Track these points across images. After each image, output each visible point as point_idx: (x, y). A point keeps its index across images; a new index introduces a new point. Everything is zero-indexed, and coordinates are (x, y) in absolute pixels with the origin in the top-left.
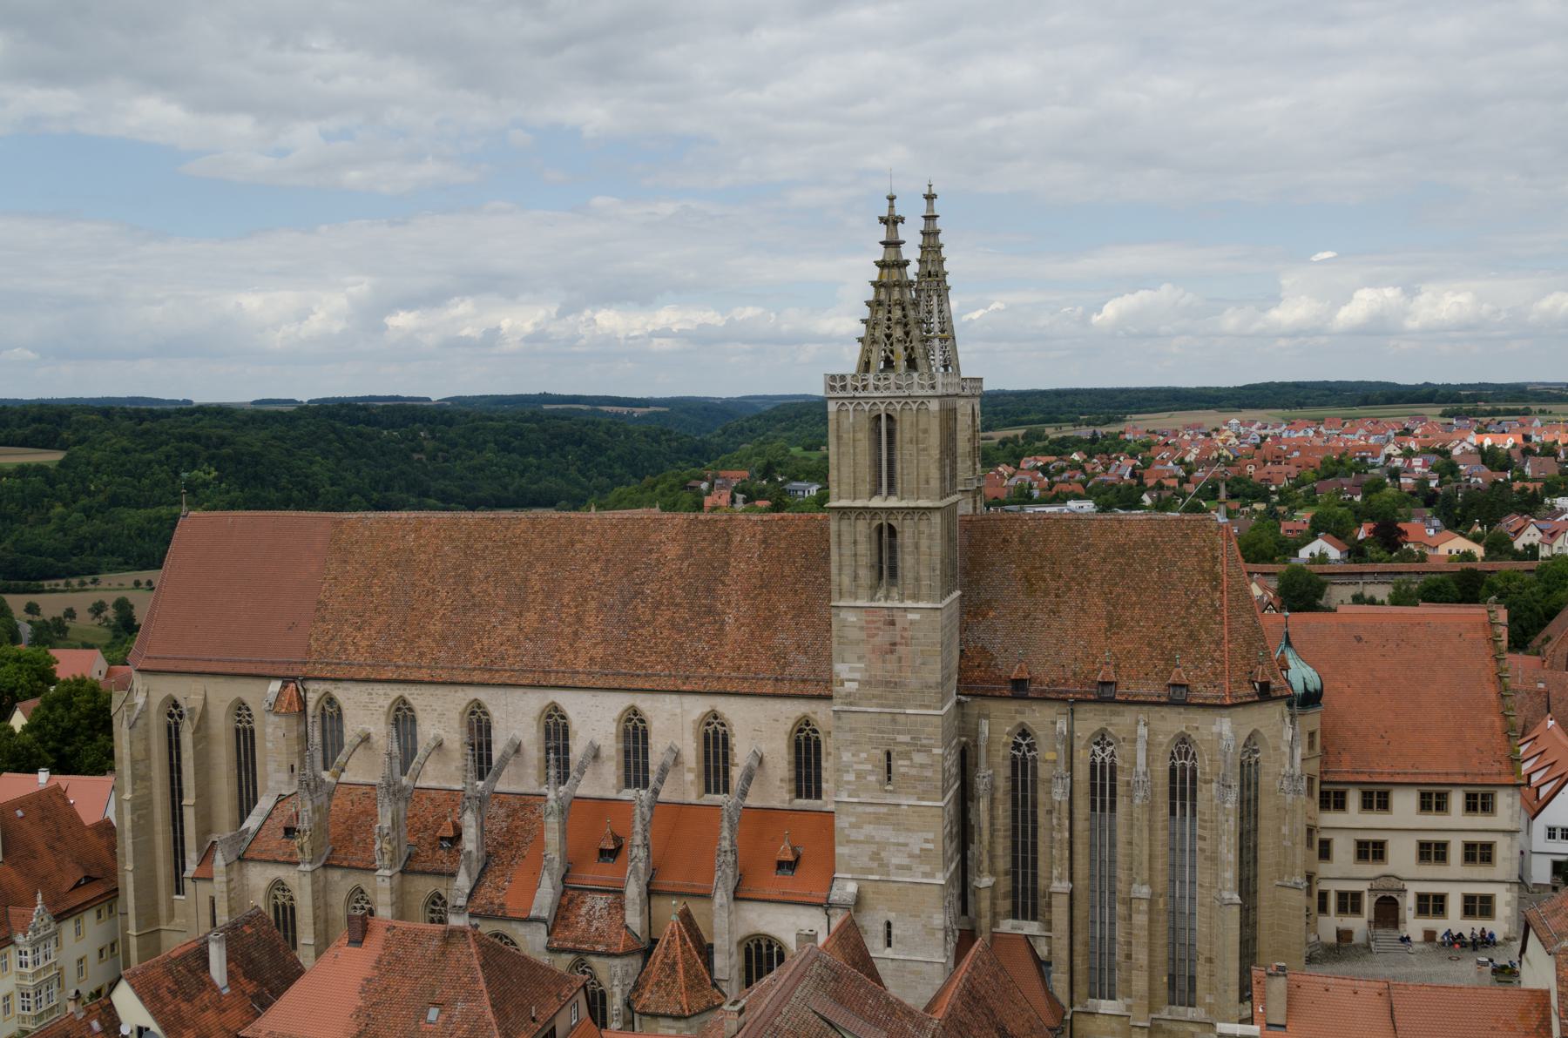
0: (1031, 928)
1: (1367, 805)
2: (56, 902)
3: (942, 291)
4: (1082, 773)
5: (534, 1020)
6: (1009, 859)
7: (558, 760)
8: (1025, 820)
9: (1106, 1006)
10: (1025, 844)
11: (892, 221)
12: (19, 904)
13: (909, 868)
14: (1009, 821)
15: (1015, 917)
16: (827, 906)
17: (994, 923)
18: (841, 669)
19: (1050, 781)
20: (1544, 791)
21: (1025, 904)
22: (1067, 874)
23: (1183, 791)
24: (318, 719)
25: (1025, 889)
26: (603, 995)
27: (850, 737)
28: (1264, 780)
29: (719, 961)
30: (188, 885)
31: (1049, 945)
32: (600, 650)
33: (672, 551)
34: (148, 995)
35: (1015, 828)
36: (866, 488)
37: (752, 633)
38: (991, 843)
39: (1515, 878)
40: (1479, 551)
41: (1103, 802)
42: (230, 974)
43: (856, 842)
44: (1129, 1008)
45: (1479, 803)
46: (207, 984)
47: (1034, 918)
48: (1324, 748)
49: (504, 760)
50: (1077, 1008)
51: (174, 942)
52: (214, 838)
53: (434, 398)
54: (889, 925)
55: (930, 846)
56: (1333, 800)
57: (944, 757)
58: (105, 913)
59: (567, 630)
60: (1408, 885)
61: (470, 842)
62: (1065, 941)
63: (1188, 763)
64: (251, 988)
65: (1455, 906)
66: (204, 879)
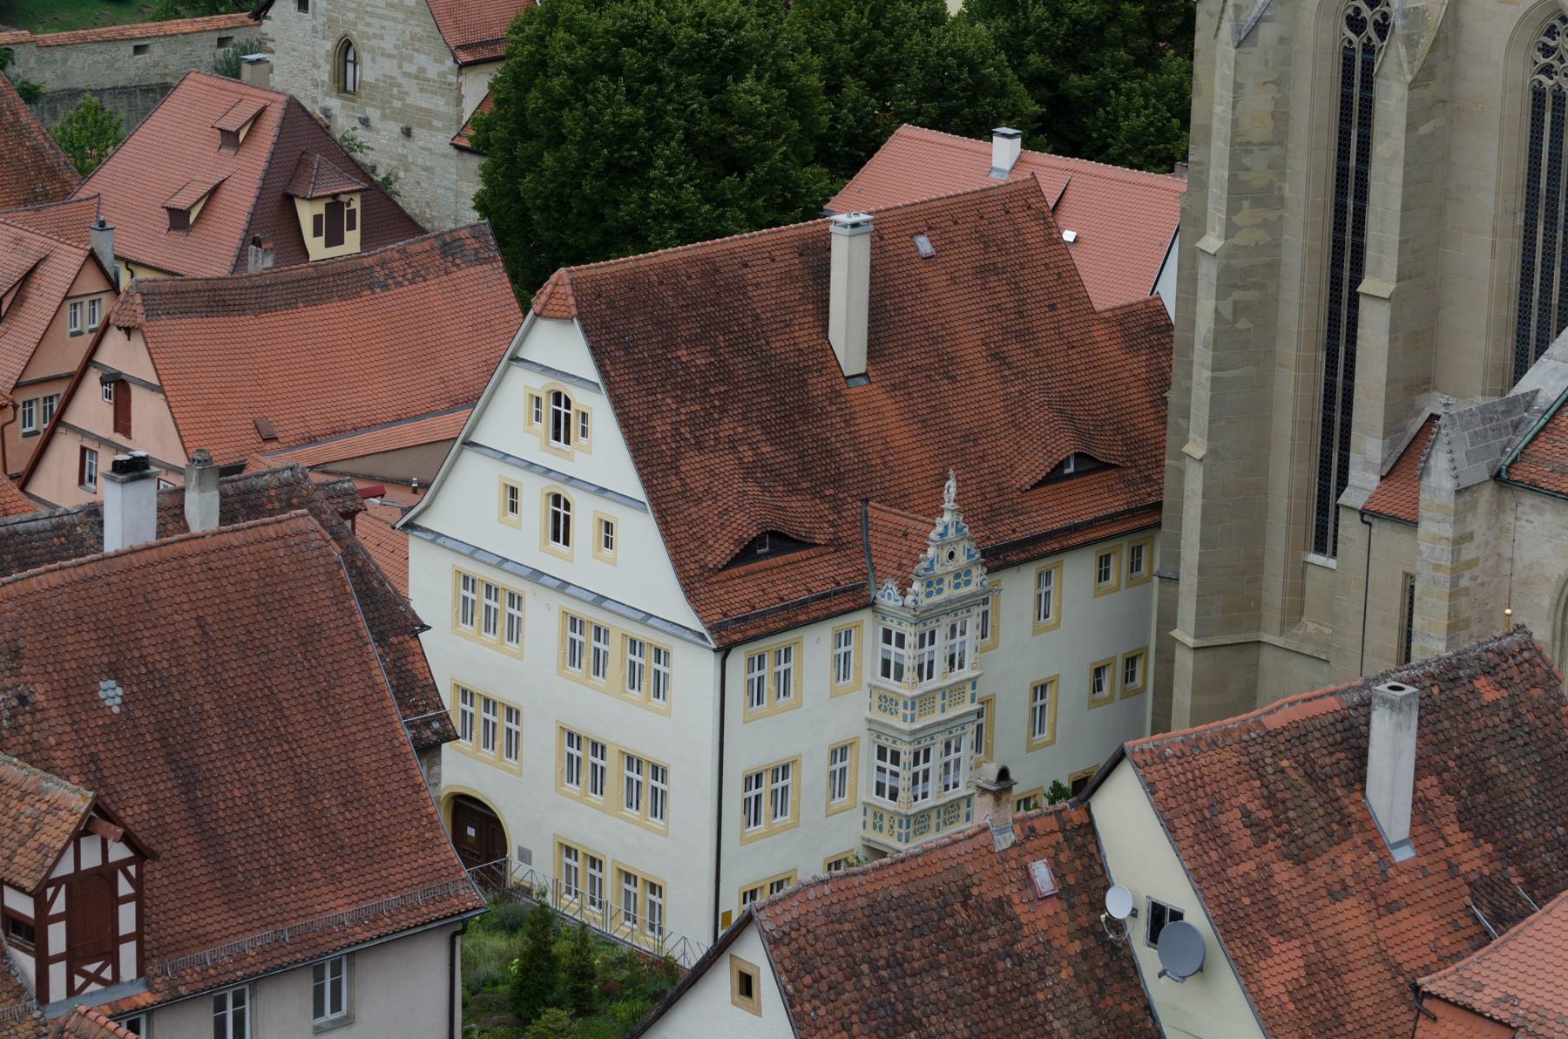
2: (993, 515)
12: (899, 500)
30: (1350, 527)
46: (1353, 823)
52: (1435, 404)
64: (1474, 859)
66: (1394, 519)
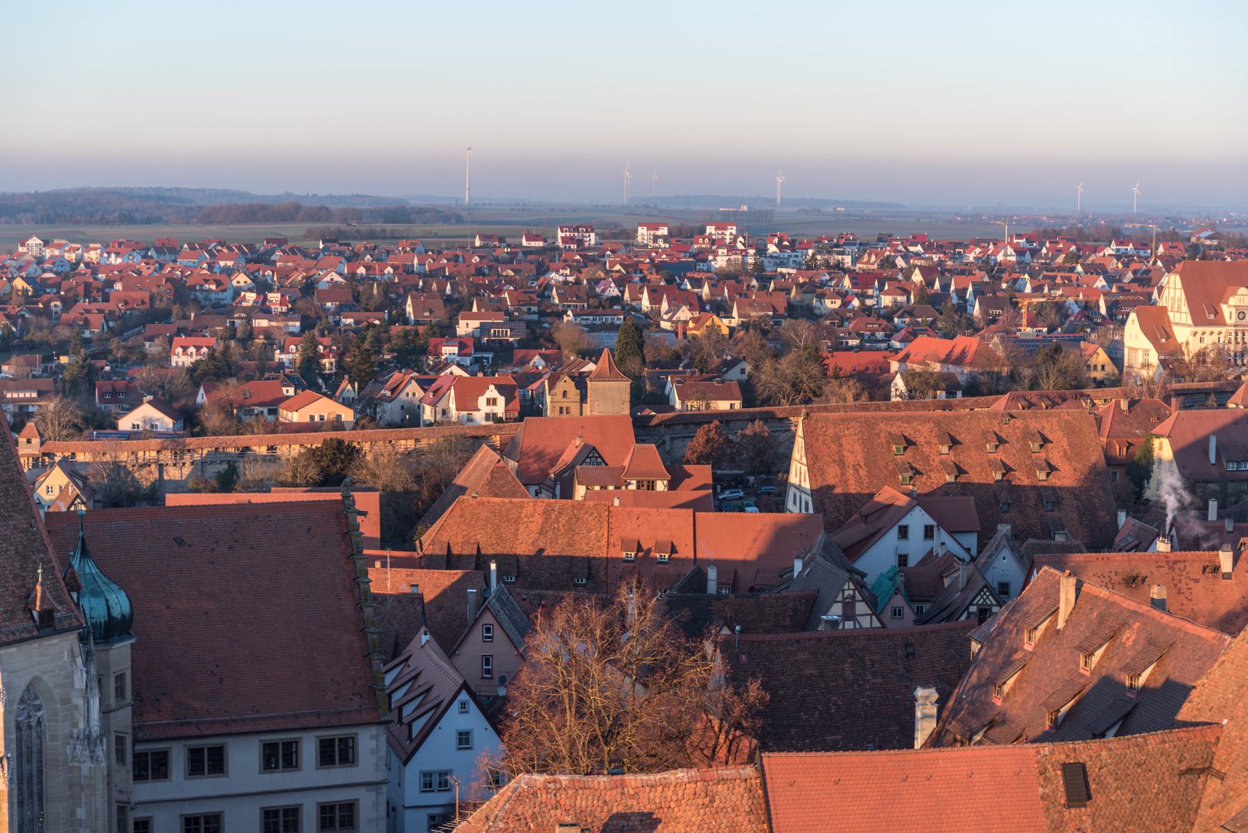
1: (195, 768)
28: (53, 746)
45: (336, 753)
48: (137, 694)
56: (151, 766)
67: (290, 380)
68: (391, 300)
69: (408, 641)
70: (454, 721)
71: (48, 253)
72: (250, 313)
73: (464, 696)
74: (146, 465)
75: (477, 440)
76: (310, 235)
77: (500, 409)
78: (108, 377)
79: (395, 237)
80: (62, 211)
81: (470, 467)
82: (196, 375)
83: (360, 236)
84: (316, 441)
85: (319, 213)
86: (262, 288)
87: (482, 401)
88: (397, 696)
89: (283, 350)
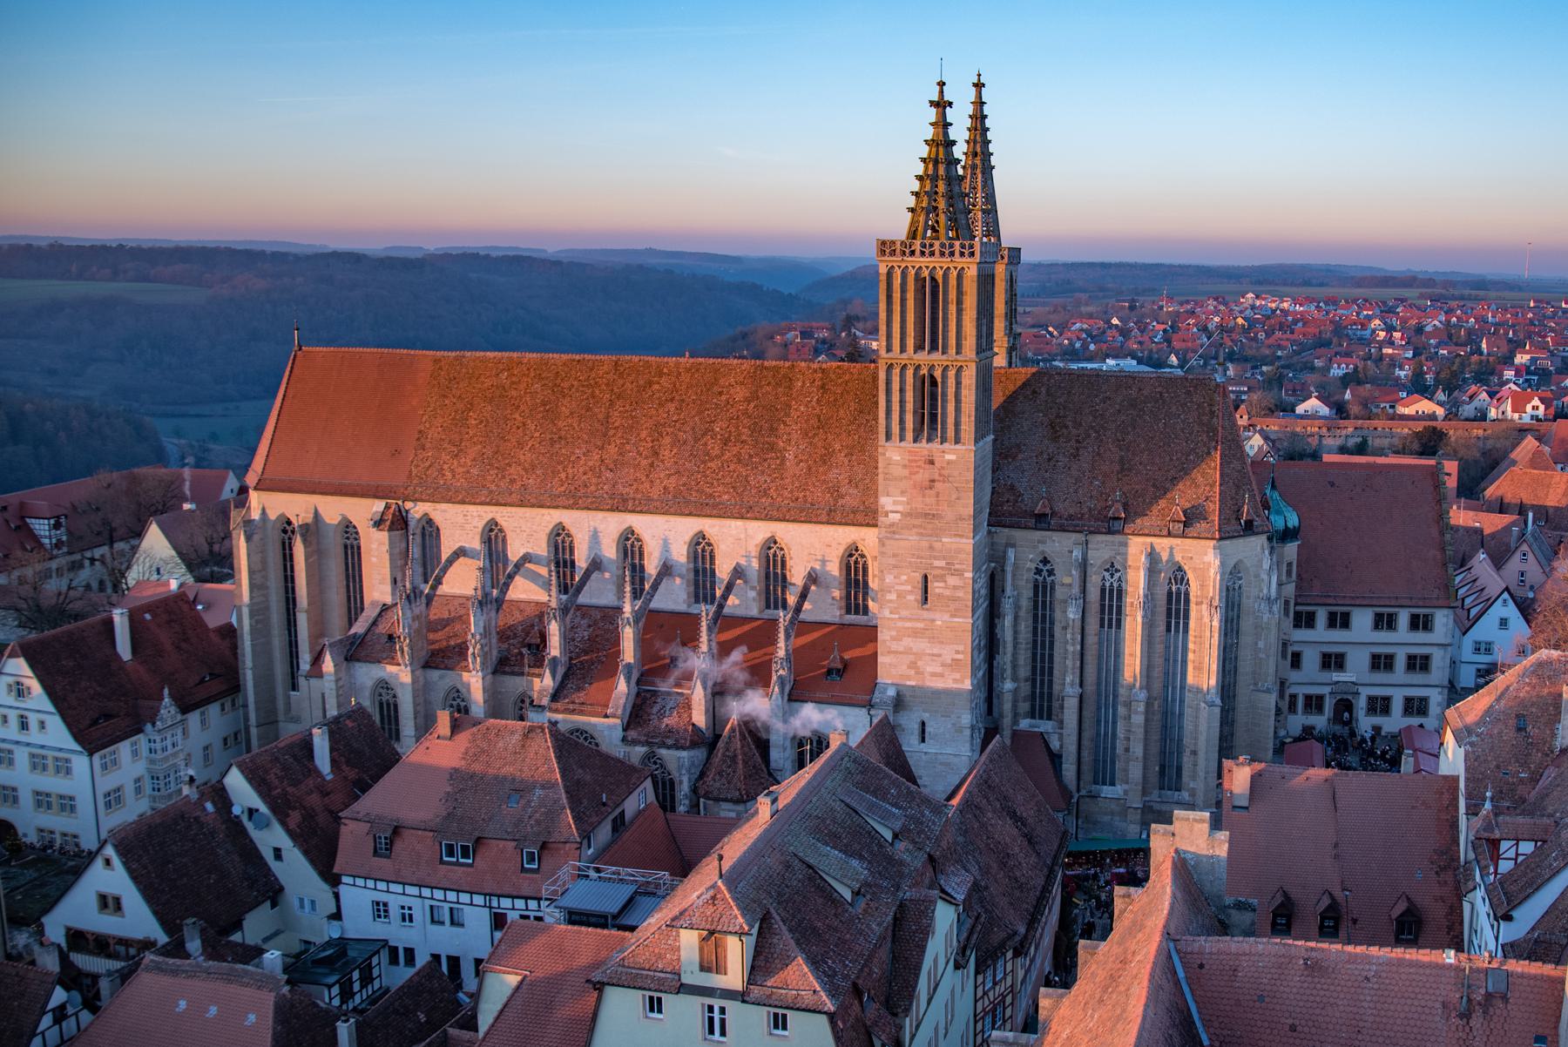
0: (1045, 726)
1: (1332, 623)
3: (988, 169)
4: (1094, 594)
5: (604, 804)
6: (1029, 668)
7: (633, 577)
8: (1043, 635)
9: (1107, 791)
10: (1043, 655)
11: (941, 105)
13: (942, 675)
14: (1030, 635)
15: (1033, 717)
16: (870, 705)
17: (1015, 722)
18: (886, 502)
19: (1065, 602)
20: (1474, 612)
21: (1041, 706)
22: (1077, 681)
23: (1177, 611)
24: (418, 539)
25: (1042, 694)
26: (672, 782)
27: (892, 561)
28: (1247, 602)
29: (774, 754)
30: (302, 682)
31: (1061, 739)
32: (673, 480)
33: (740, 393)
34: (256, 778)
35: (1035, 642)
36: (910, 342)
37: (810, 468)
38: (1014, 655)
39: (1446, 683)
40: (1440, 412)
41: (1110, 620)
42: (333, 761)
43: (896, 652)
44: (1126, 792)
45: (1420, 623)
47: (1049, 718)
48: (1299, 575)
49: (587, 575)
50: (1083, 792)
51: (289, 732)
53: (550, 250)
54: (923, 724)
55: (960, 657)
56: (1304, 620)
57: (974, 581)
58: (228, 706)
59: (644, 462)
60: (1361, 689)
61: (555, 648)
62: (1074, 738)
63: (1183, 588)
64: (352, 774)
65: (1397, 706)
67: (1403, 387)
68: (1472, 339)
69: (1471, 557)
70: (1497, 611)
71: (1258, 303)
72: (1381, 345)
73: (1506, 595)
74: (1312, 435)
75: (1523, 431)
76: (1422, 296)
77: (1541, 412)
78: (1291, 380)
79: (1476, 299)
80: (1269, 278)
81: (1519, 449)
82: (1346, 381)
83: (1454, 298)
84: (1419, 427)
85: (1429, 282)
86: (1390, 329)
87: (1529, 408)
88: (1461, 592)
89: (1401, 369)
